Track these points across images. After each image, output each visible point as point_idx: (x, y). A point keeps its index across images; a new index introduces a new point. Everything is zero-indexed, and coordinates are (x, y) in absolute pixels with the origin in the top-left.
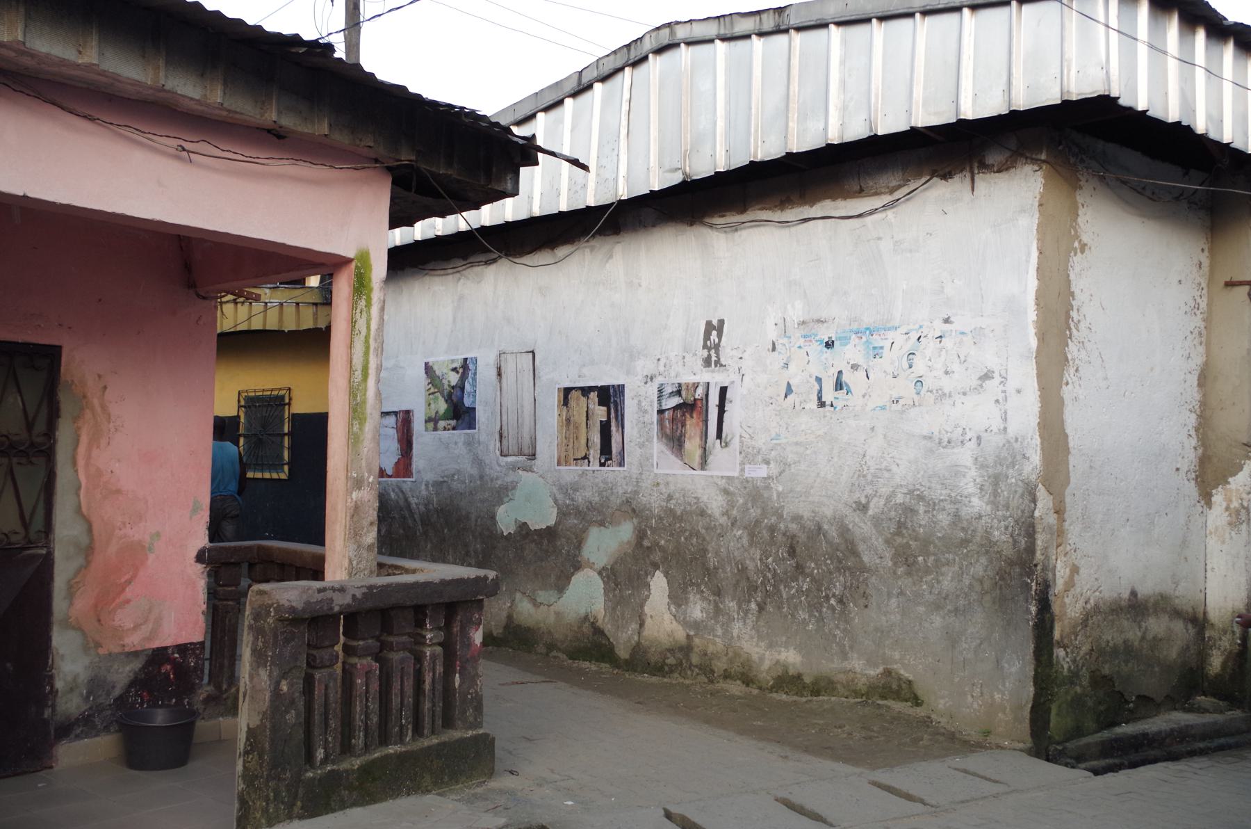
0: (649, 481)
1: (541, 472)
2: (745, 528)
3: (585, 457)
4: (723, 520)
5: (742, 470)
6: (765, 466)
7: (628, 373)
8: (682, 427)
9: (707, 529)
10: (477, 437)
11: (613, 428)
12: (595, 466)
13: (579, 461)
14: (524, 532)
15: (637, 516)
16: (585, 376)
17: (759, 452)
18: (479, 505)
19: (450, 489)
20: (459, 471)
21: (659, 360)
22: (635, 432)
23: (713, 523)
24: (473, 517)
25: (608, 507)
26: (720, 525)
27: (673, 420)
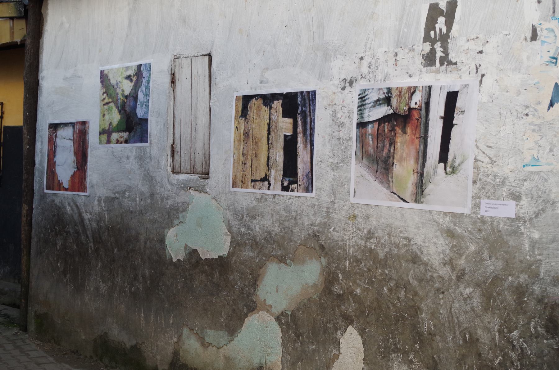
0: (343, 212)
1: (214, 194)
2: (478, 285)
3: (265, 179)
4: (445, 271)
5: (477, 206)
6: (513, 203)
7: (321, 77)
8: (391, 145)
9: (420, 281)
10: (148, 151)
11: (300, 145)
12: (278, 191)
13: (258, 183)
14: (194, 261)
15: (326, 255)
16: (268, 82)
17: (503, 183)
18: (148, 226)
19: (120, 204)
20: (130, 187)
21: (361, 59)
22: (327, 150)
23: (429, 274)
24: (142, 238)
25: (291, 241)
26: (440, 277)
27: (378, 136)
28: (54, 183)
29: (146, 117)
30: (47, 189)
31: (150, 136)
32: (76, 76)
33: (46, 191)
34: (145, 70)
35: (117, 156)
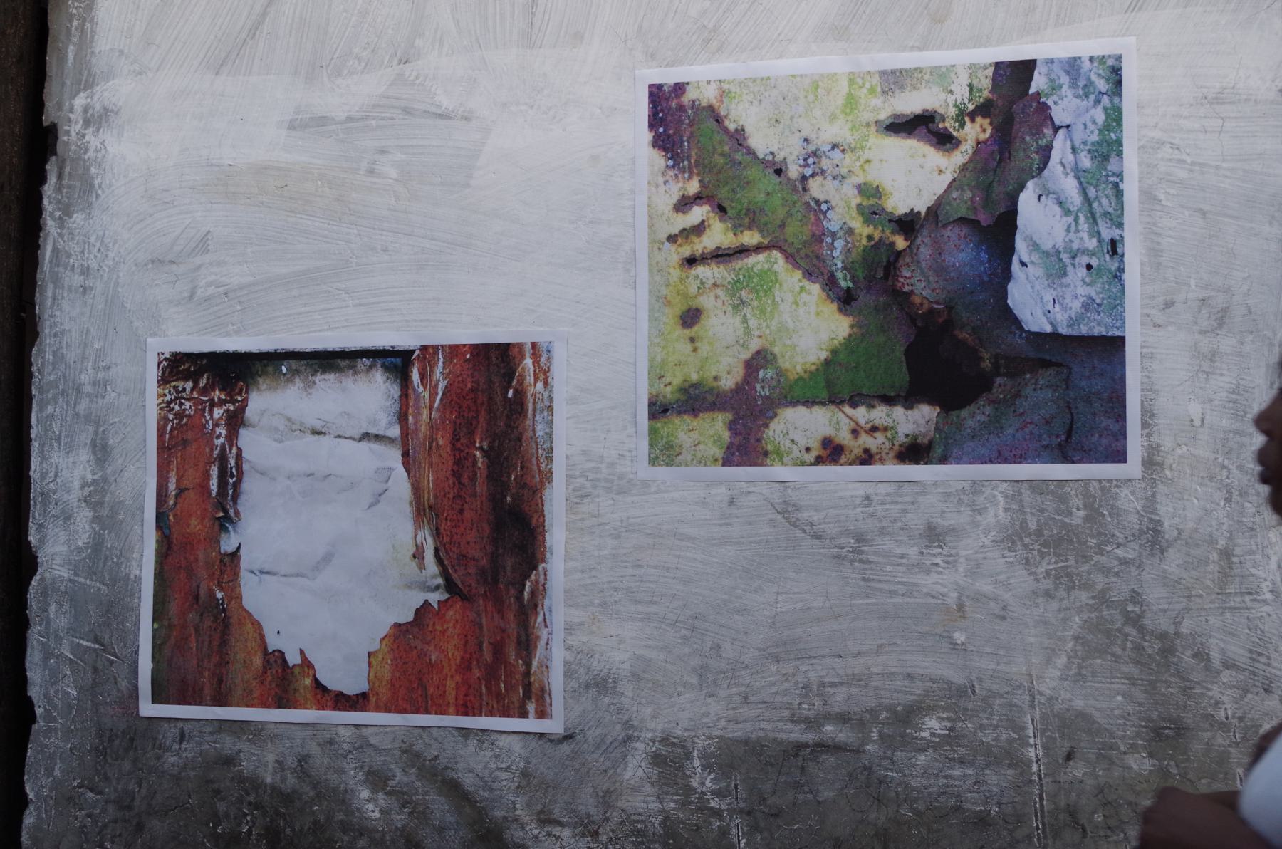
10: (1129, 501)
28: (224, 662)
29: (1118, 333)
30: (157, 698)
31: (1145, 425)
32: (406, 111)
33: (148, 709)
34: (1066, 90)
35: (832, 529)
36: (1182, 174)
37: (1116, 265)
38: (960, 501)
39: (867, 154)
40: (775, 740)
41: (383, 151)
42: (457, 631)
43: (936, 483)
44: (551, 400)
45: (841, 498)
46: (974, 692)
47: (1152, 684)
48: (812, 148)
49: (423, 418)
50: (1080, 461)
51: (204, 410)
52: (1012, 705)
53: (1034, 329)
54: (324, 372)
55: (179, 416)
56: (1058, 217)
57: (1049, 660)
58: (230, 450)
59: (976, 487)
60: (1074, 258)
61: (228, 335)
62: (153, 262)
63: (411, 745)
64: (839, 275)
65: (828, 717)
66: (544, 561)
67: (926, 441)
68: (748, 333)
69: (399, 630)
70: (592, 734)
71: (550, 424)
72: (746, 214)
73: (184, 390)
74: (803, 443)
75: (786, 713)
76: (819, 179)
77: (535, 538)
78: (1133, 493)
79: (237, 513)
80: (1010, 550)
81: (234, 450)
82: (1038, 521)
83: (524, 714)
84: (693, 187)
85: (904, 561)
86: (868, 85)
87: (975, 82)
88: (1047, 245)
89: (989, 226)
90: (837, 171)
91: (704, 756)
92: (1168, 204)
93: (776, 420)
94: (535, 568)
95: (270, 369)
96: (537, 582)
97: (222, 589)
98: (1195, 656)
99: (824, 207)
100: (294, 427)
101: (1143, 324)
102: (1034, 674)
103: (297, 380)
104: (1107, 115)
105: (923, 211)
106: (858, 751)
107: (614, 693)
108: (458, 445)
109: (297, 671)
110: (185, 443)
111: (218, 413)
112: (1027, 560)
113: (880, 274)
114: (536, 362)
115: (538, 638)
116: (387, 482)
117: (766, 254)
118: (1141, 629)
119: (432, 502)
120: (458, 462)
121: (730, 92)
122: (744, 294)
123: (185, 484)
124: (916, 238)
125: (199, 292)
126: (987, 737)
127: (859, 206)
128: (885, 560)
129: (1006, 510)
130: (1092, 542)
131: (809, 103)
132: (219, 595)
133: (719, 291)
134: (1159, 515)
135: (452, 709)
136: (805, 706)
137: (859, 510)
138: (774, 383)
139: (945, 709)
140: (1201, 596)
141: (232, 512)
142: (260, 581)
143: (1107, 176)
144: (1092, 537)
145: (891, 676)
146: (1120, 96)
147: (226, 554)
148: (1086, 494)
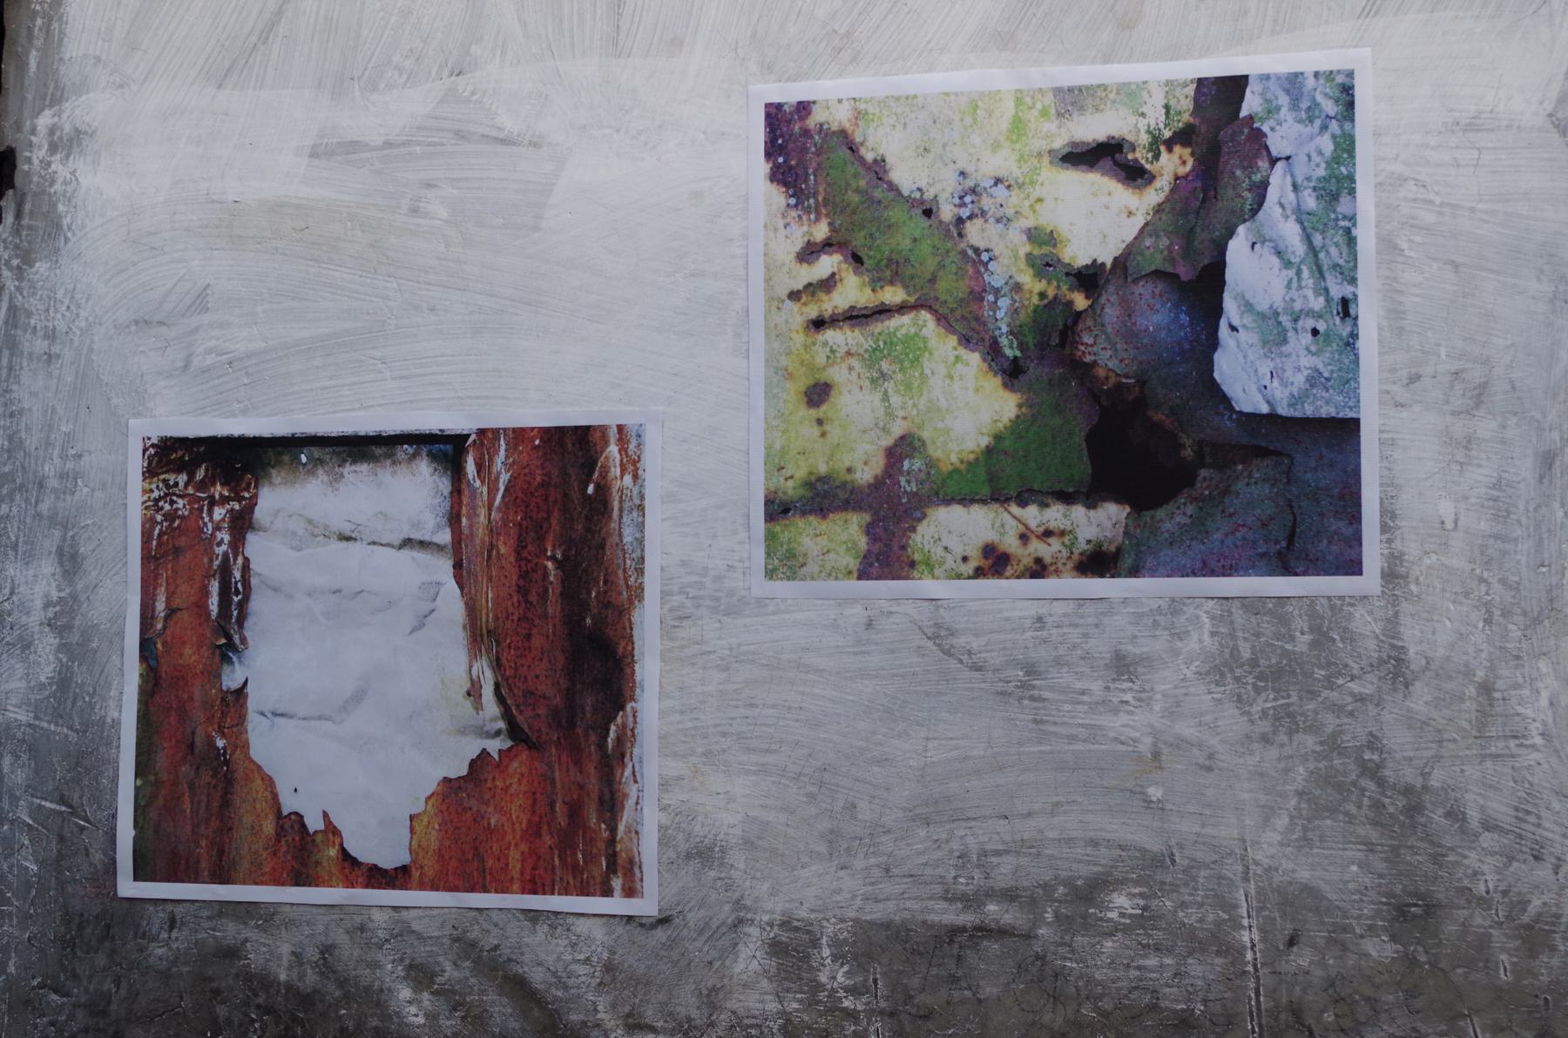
10: (1366, 624)
28: (226, 828)
29: (1351, 415)
30: (140, 874)
31: (1384, 528)
32: (459, 135)
33: (128, 887)
35: (994, 658)
36: (1429, 218)
37: (1349, 329)
38: (1156, 624)
39: (1038, 192)
40: (924, 922)
41: (429, 185)
42: (523, 788)
43: (1125, 601)
44: (642, 498)
45: (1007, 620)
46: (1173, 862)
47: (1395, 850)
48: (970, 183)
49: (479, 521)
50: (1305, 573)
51: (201, 510)
52: (1221, 878)
53: (1247, 409)
54: (354, 462)
55: (170, 517)
56: (1276, 270)
57: (1266, 821)
58: (235, 559)
59: (1176, 605)
60: (1296, 320)
61: (233, 415)
62: (136, 322)
63: (465, 932)
64: (1004, 341)
65: (990, 894)
66: (632, 699)
67: (1113, 548)
68: (890, 414)
69: (450, 788)
70: (694, 917)
71: (641, 526)
72: (887, 266)
73: (176, 484)
74: (959, 550)
75: (938, 889)
76: (978, 222)
77: (622, 670)
78: (1370, 613)
79: (244, 640)
80: (1217, 684)
81: (240, 560)
82: (1253, 648)
83: (607, 892)
84: (821, 231)
85: (1085, 698)
86: (1039, 106)
87: (1172, 103)
88: (1263, 305)
89: (1190, 281)
90: (1000, 212)
91: (836, 943)
92: (1412, 254)
93: (925, 522)
94: (622, 708)
95: (286, 458)
96: (624, 726)
97: (223, 735)
98: (1448, 815)
99: (985, 257)
100: (316, 531)
101: (1381, 403)
102: (1248, 838)
103: (320, 472)
104: (1337, 145)
105: (1109, 265)
106: (1028, 936)
107: (722, 865)
108: (525, 554)
109: (319, 838)
110: (177, 551)
111: (219, 513)
112: (1239, 696)
113: (1055, 340)
114: (623, 450)
115: (626, 796)
116: (434, 600)
117: (912, 315)
118: (1381, 783)
119: (492, 625)
120: (524, 575)
121: (867, 113)
122: (885, 365)
123: (177, 602)
124: (1099, 296)
125: (196, 361)
126: (1190, 917)
127: (1029, 256)
128: (1062, 697)
129: (1213, 634)
130: (1320, 673)
131: (965, 128)
132: (220, 743)
133: (854, 362)
134: (1401, 639)
135: (516, 886)
136: (962, 880)
137: (1029, 634)
138: (923, 476)
139: (1137, 883)
140: (1455, 741)
141: (236, 638)
142: (273, 725)
143: (1337, 219)
144: (1321, 667)
145: (1070, 841)
146: (1352, 120)
147: (228, 692)
148: (1313, 615)
